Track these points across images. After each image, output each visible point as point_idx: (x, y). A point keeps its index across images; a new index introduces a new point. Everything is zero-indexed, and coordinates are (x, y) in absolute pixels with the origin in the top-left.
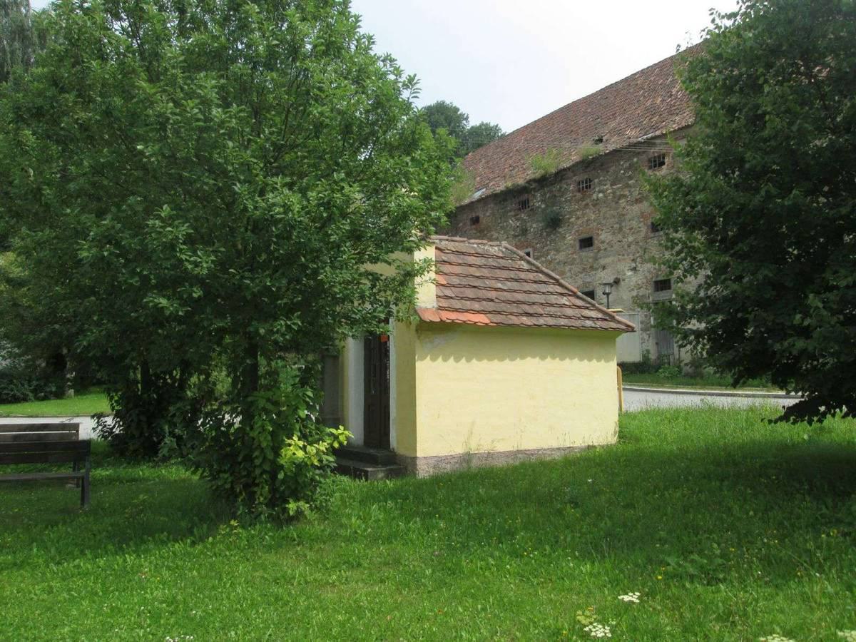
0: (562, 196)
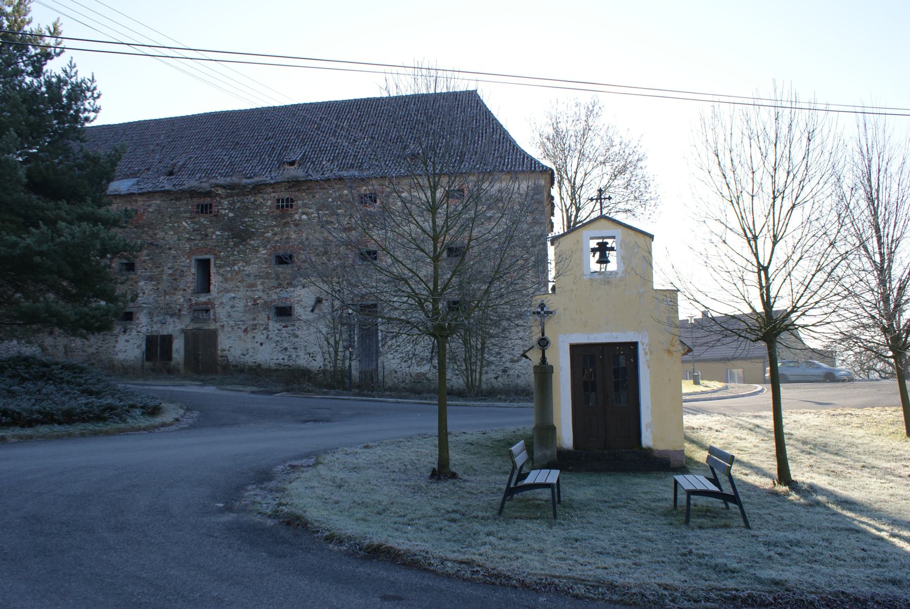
0: (257, 209)
